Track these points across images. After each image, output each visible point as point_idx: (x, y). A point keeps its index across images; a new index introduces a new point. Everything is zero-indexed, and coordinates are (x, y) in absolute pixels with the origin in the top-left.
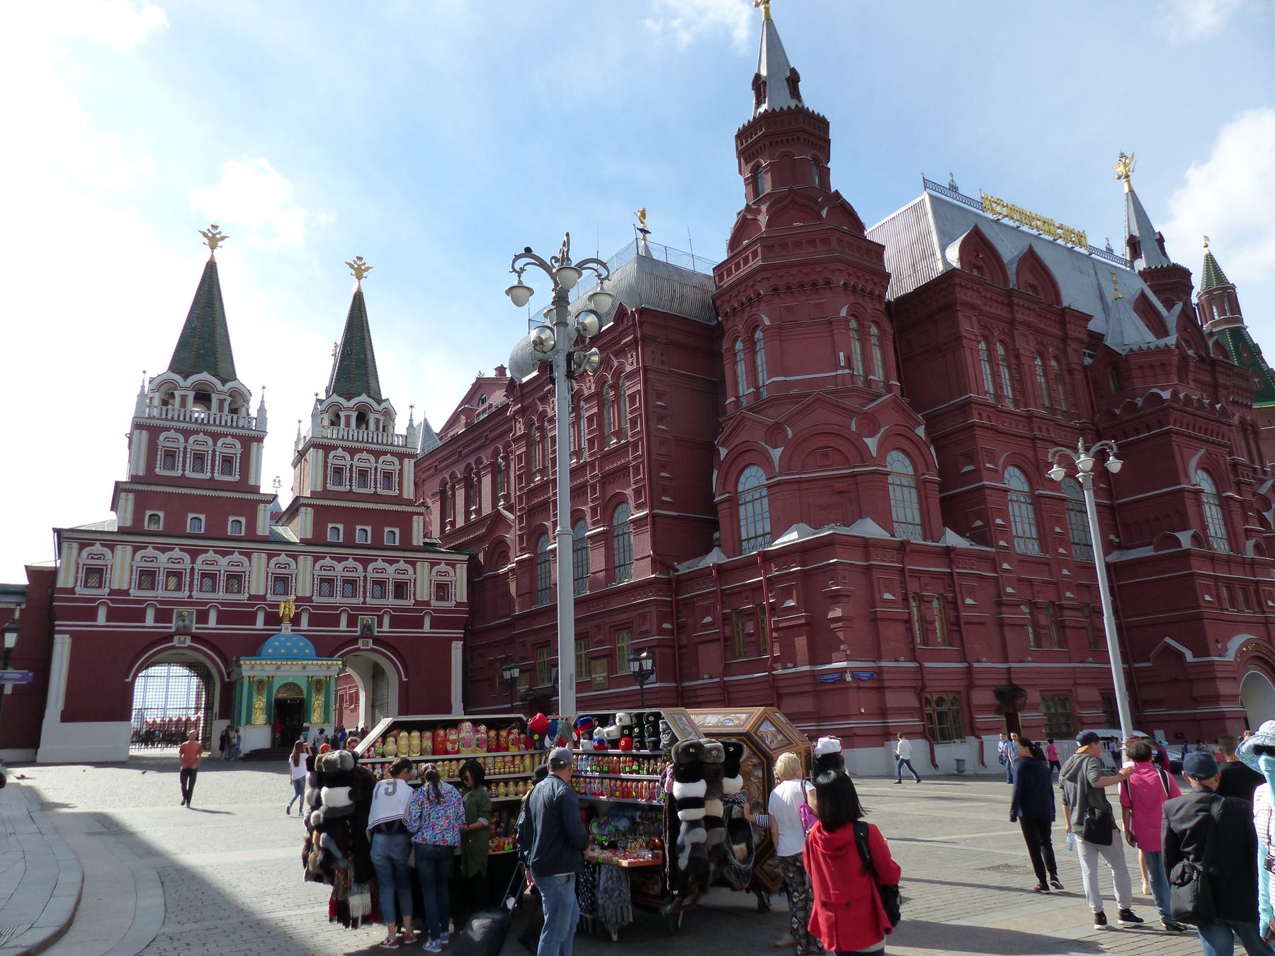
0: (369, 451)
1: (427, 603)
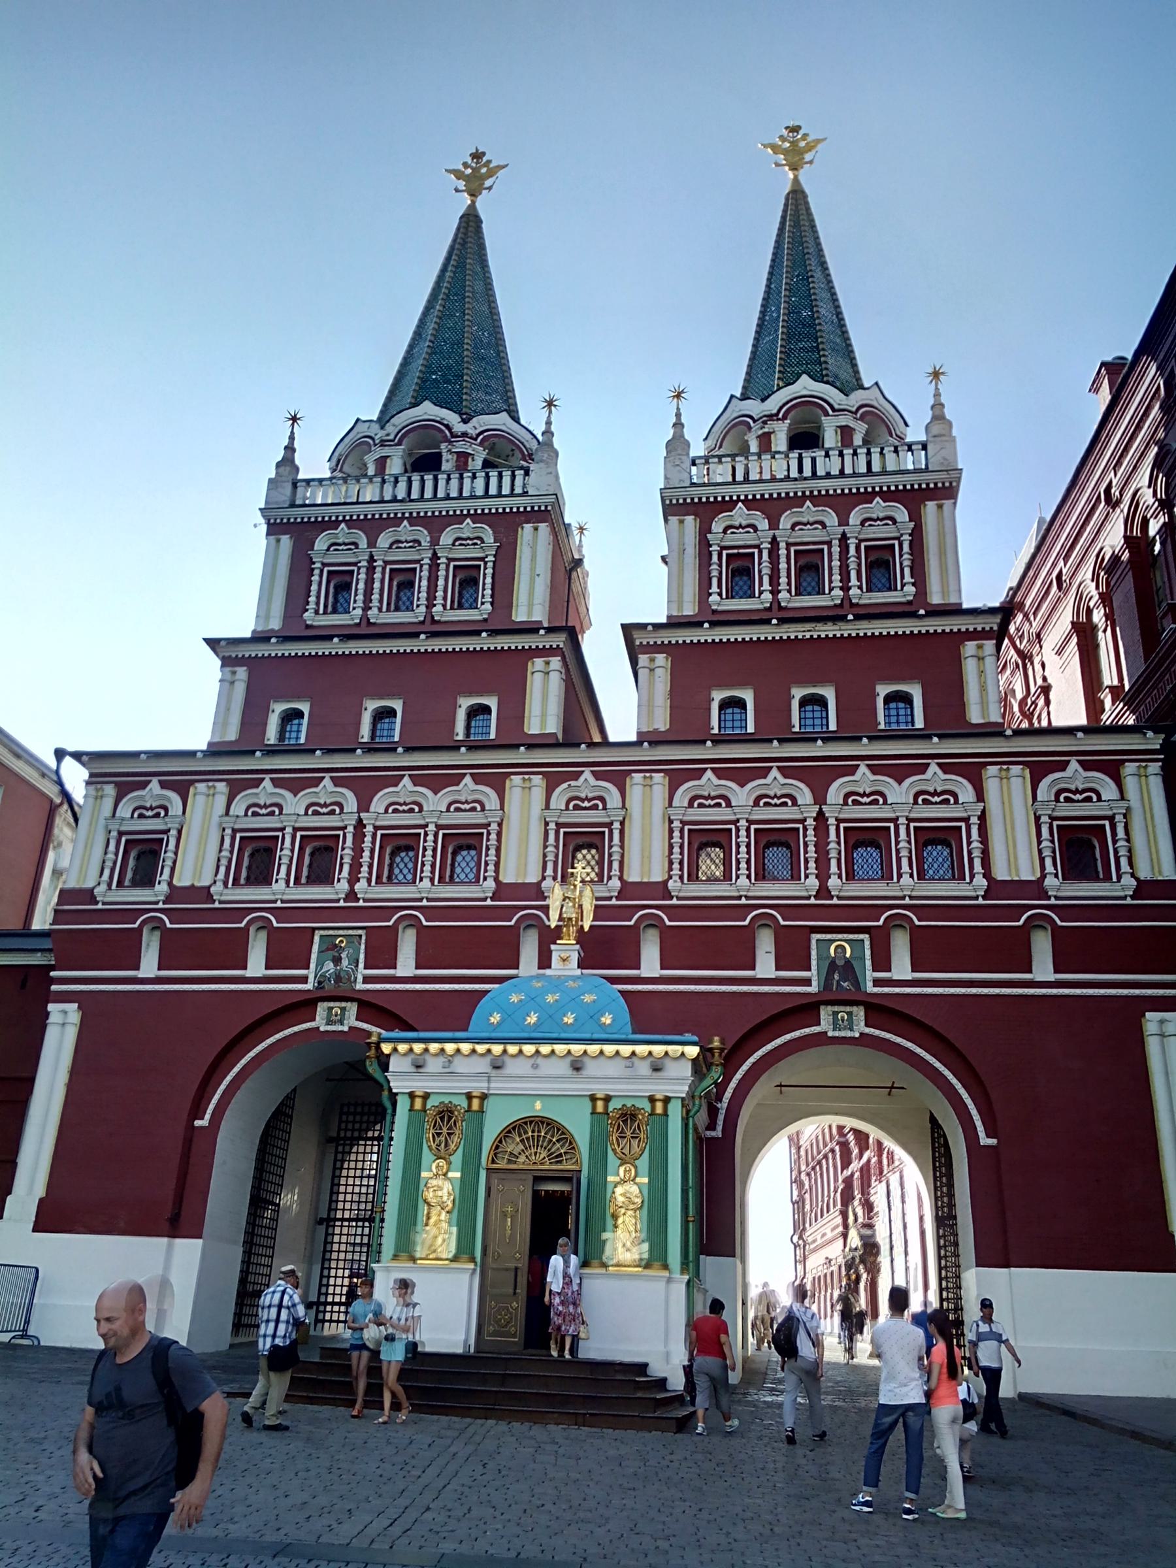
0: (819, 499)
1: (1037, 888)
